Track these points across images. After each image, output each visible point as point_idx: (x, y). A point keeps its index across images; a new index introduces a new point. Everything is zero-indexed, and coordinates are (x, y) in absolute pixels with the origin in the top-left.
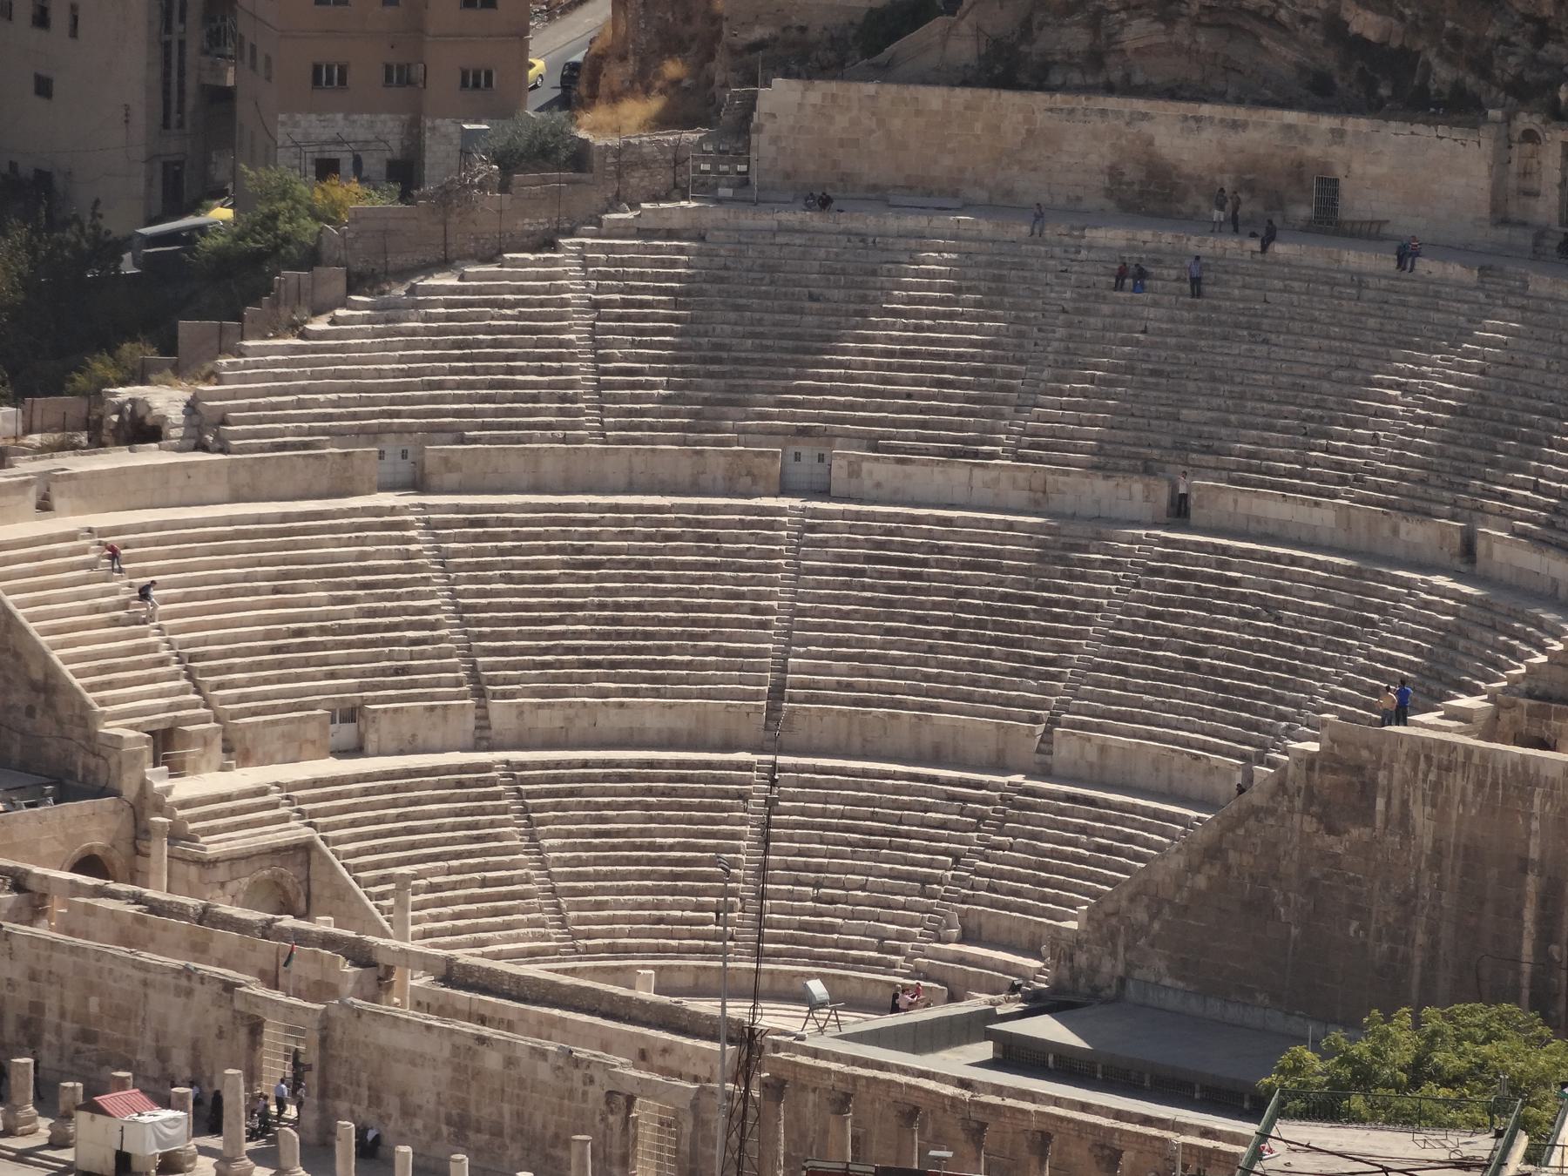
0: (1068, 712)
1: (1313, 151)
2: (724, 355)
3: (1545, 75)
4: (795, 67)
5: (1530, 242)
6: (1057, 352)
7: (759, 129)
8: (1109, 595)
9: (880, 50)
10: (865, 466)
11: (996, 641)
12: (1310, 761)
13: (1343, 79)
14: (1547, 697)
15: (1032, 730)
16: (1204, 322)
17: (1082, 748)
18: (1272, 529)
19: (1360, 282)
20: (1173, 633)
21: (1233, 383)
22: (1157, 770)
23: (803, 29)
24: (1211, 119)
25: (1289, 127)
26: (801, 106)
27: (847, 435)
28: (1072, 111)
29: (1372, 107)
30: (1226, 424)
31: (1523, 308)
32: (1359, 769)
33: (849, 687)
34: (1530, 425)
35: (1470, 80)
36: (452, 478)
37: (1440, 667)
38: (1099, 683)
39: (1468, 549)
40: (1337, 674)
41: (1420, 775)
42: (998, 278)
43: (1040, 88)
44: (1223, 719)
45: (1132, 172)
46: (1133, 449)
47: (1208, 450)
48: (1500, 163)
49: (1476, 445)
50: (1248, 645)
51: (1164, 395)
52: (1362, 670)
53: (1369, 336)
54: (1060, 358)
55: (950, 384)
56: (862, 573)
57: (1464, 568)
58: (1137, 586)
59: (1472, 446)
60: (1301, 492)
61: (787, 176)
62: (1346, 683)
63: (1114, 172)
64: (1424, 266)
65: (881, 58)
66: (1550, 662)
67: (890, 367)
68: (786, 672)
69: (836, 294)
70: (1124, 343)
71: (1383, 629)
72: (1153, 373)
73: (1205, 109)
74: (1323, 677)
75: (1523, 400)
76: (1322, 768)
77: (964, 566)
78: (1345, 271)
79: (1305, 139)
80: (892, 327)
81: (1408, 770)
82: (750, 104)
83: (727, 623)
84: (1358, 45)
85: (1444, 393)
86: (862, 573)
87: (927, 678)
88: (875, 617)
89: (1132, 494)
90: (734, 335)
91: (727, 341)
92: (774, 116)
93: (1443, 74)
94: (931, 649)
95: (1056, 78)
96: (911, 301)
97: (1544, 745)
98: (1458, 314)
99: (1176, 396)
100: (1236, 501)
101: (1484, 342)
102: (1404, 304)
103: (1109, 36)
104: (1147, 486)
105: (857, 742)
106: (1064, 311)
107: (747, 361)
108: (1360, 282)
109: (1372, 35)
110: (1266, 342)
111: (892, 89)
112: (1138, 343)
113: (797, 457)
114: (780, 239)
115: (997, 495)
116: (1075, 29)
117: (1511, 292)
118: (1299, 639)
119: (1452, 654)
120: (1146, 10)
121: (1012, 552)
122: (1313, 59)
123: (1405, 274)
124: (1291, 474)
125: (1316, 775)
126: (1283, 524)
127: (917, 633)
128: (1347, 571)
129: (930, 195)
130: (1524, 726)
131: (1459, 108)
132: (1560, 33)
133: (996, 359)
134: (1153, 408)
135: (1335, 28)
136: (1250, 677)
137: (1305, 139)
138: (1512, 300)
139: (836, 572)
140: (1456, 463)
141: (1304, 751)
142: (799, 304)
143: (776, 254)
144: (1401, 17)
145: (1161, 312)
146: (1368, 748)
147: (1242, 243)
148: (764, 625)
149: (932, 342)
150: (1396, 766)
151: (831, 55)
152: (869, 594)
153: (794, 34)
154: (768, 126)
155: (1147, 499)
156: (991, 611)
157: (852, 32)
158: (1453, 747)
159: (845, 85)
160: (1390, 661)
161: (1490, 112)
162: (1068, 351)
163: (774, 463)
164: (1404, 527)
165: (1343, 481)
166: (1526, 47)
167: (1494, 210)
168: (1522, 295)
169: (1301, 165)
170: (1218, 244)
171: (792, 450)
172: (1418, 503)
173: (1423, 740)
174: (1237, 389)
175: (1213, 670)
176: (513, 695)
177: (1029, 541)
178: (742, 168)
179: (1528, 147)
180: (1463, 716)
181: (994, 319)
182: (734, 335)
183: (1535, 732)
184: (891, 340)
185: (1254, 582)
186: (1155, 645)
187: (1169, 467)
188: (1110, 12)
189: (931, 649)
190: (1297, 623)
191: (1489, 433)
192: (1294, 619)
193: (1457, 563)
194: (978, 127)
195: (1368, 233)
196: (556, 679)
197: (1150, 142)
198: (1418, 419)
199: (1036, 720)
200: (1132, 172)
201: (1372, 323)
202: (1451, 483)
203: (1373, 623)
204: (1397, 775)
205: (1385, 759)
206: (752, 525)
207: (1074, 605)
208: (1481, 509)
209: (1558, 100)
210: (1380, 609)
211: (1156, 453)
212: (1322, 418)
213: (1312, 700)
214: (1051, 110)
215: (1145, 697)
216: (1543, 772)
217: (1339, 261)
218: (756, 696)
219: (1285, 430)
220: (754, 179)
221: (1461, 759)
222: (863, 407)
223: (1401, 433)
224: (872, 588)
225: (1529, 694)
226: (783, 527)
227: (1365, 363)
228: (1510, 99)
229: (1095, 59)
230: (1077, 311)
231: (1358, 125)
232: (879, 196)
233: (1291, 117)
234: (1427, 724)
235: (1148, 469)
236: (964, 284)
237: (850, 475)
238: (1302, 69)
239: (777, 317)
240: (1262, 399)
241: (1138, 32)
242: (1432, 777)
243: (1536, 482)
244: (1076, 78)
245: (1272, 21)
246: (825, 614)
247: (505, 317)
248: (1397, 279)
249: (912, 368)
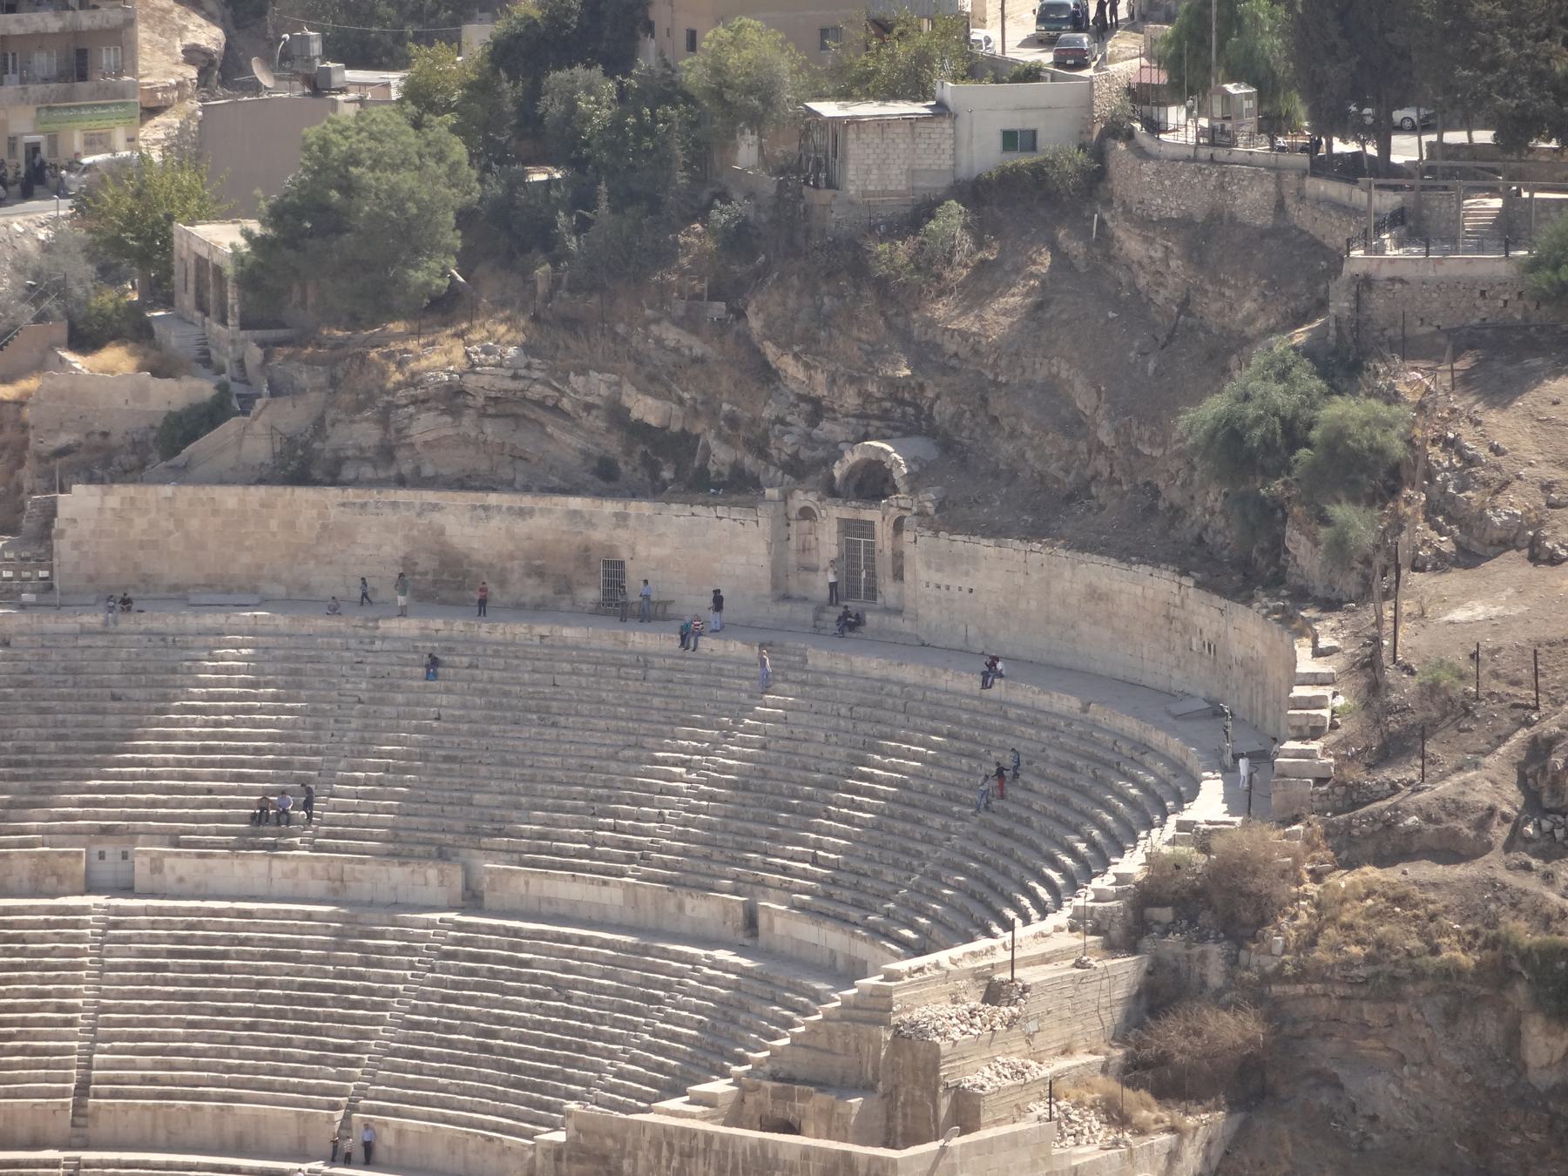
0: (366, 1098)
1: (599, 535)
2: (27, 757)
3: (820, 453)
4: (98, 472)
5: (810, 617)
6: (353, 743)
7: (61, 533)
8: (404, 980)
9: (177, 452)
10: (168, 862)
11: (296, 1030)
12: (557, 1152)
13: (626, 463)
14: (791, 1079)
15: (330, 1117)
16: (495, 707)
18: (563, 909)
19: (646, 662)
20: (468, 1017)
21: (524, 766)
22: (453, 1153)
23: (105, 435)
24: (499, 508)
25: (574, 514)
26: (101, 510)
27: (150, 832)
28: (364, 505)
29: (655, 490)
30: (518, 807)
31: (803, 683)
32: (604, 1158)
33: (154, 1081)
34: (809, 798)
35: (749, 461)
37: (721, 1042)
38: (396, 1068)
39: (751, 922)
40: (624, 1052)
41: (664, 1162)
42: (295, 672)
43: (333, 484)
44: (516, 1100)
45: (425, 563)
46: (428, 835)
47: (500, 833)
48: (779, 541)
49: (757, 819)
50: (539, 1025)
51: (456, 780)
52: (648, 1047)
53: (655, 716)
54: (355, 748)
55: (250, 778)
56: (165, 968)
57: (747, 942)
58: (432, 970)
59: (754, 820)
60: (590, 872)
61: (90, 579)
62: (631, 1061)
63: (408, 563)
64: (708, 644)
65: (178, 460)
66: (792, 1044)
67: (190, 763)
68: (90, 1067)
69: (138, 693)
70: (418, 730)
71: (669, 1005)
72: (447, 759)
73: (493, 499)
74: (611, 1055)
75: (803, 774)
76: (569, 1159)
77: (265, 957)
78: (630, 652)
79: (590, 524)
80: (193, 723)
81: (651, 1157)
82: (51, 511)
83: (34, 1022)
84: (640, 430)
85: (726, 769)
86: (165, 968)
87: (229, 1069)
88: (179, 1010)
89: (429, 878)
90: (38, 738)
91: (28, 743)
92: (74, 521)
93: (722, 456)
94: (233, 1040)
95: (348, 473)
96: (211, 697)
97: (790, 1128)
98: (740, 690)
99: (468, 781)
100: (527, 883)
101: (764, 718)
102: (687, 682)
103: (399, 431)
104: (441, 871)
105: (161, 1135)
106: (360, 701)
107: (51, 764)
108: (646, 662)
109: (653, 420)
110: (554, 725)
111: (189, 490)
112: (431, 731)
113: (102, 856)
114: (81, 642)
115: (296, 885)
116: (365, 425)
117: (790, 668)
118: (587, 1018)
119: (733, 1028)
120: (432, 404)
121: (311, 941)
122: (598, 445)
123: (689, 653)
124: (580, 854)
125: (564, 1166)
126: (574, 904)
127: (219, 1026)
128: (632, 949)
129: (229, 592)
130: (769, 1107)
131: (738, 487)
132: (834, 411)
133: (293, 752)
134: (446, 794)
135: (617, 415)
136: (541, 1058)
137: (590, 524)
138: (791, 675)
139: (140, 967)
140: (738, 838)
141: (551, 1142)
142: (102, 704)
143: (79, 657)
144: (681, 401)
145: (453, 699)
146: (612, 1136)
147: (531, 628)
148: (70, 1023)
149: (231, 737)
150: (640, 1154)
151: (133, 459)
152: (171, 989)
153: (97, 439)
154: (70, 531)
155: (441, 884)
156: (290, 1000)
157: (153, 435)
158: (693, 1134)
159: (142, 488)
160: (675, 1037)
161: (768, 491)
162: (363, 741)
163: (79, 862)
164: (689, 903)
165: (630, 860)
166: (800, 425)
167: (775, 587)
168: (803, 670)
170: (508, 630)
171: (96, 849)
172: (701, 879)
173: (665, 1128)
174: (527, 771)
175: (506, 1051)
177: (326, 931)
178: (43, 574)
179: (806, 523)
180: (708, 1101)
181: (291, 711)
182: (38, 738)
183: (779, 1114)
184: (192, 736)
185: (545, 962)
186: (450, 1029)
187: (464, 852)
188: (398, 407)
189: (233, 1040)
190: (586, 1002)
191: (763, 807)
192: (582, 997)
193: (741, 938)
194: (274, 524)
195: (650, 612)
197: (442, 533)
198: (701, 796)
199: (335, 1107)
200: (425, 563)
201: (657, 702)
202: (733, 858)
203: (659, 1000)
204: (642, 1163)
205: (629, 1147)
206: (57, 925)
207: (370, 992)
208: (761, 883)
209: (832, 477)
210: (666, 986)
211: (449, 838)
212: (609, 797)
213: (600, 1078)
214: (344, 505)
215: (441, 1080)
216: (781, 1156)
217: (625, 643)
218: (63, 1093)
219: (575, 810)
220: (56, 583)
221: (701, 1145)
222: (165, 804)
223: (685, 810)
224: (175, 982)
225: (774, 1077)
226: (86, 925)
227: (650, 742)
228: (787, 477)
229: (387, 453)
230: (372, 701)
231: (642, 508)
232: (180, 595)
233: (575, 503)
234: (673, 1113)
235: (442, 854)
236: (262, 679)
237: (153, 871)
238: (586, 455)
239: (81, 718)
240: (552, 781)
242: (675, 1164)
243: (815, 856)
244: (368, 472)
245: (556, 409)
246: (129, 1009)
248: (681, 658)
249: (212, 764)
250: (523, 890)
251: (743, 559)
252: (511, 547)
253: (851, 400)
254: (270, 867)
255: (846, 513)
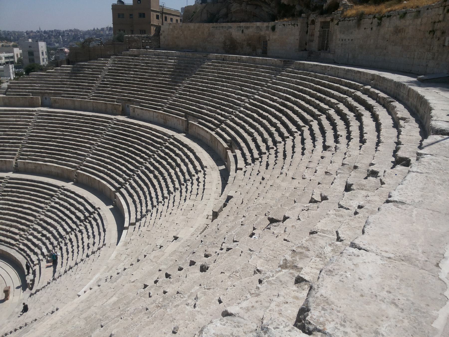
1: (262, 33)
7: (161, 35)
10: (136, 109)
25: (258, 27)
28: (217, 27)
36: (57, 105)
45: (228, 43)
63: (225, 43)
79: (261, 30)
171: (127, 105)
176: (25, 159)
196: (38, 156)
229: (226, 15)
233: (258, 24)
241: (235, 7)
247: (89, 71)
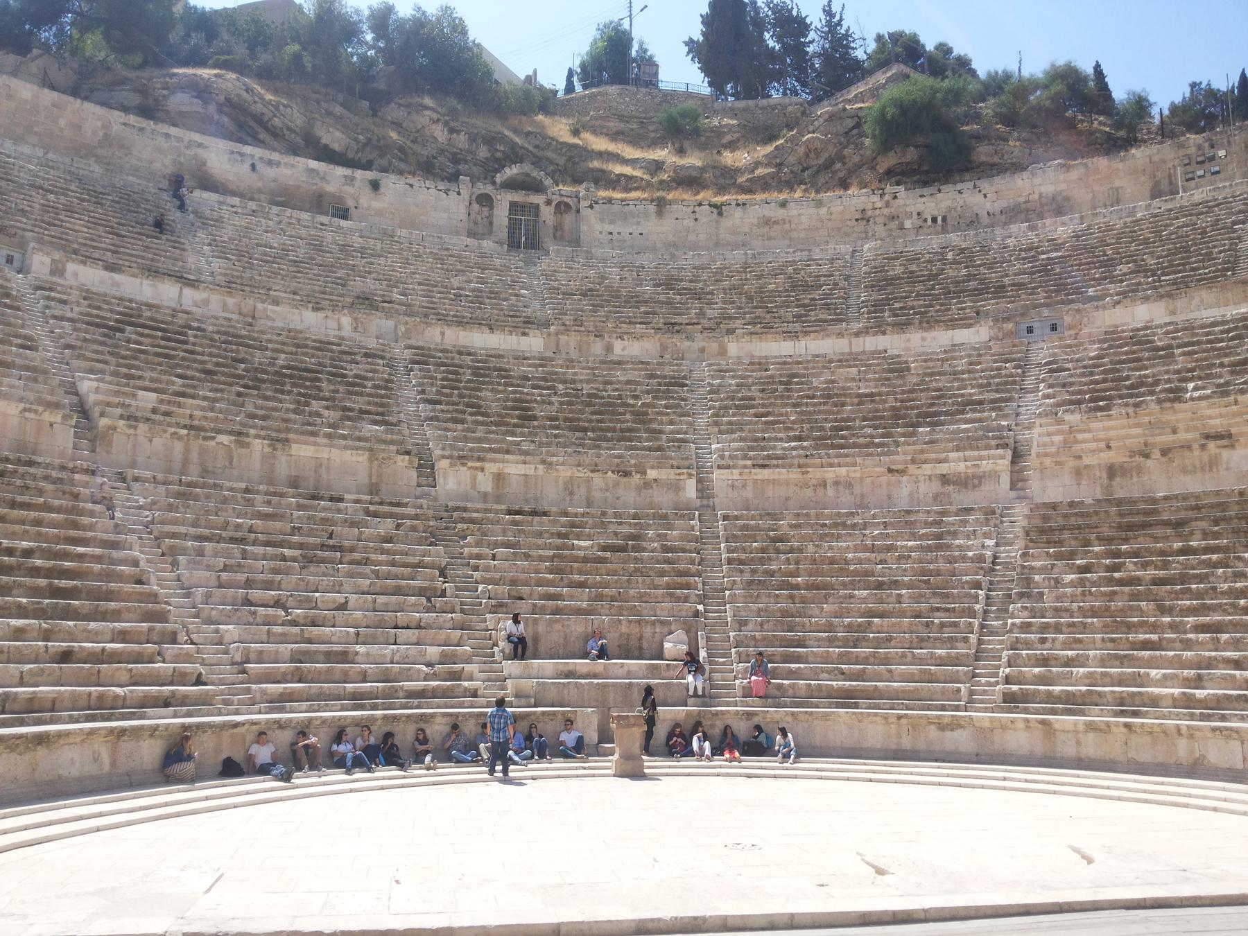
1: (330, 188)
17: (474, 479)
22: (571, 493)
25: (313, 170)
28: (142, 130)
73: (247, 149)
79: (323, 179)
100: (443, 334)
109: (336, 147)
137: (323, 179)
144: (356, 140)
169: (320, 196)
194: (62, 122)
197: (204, 164)
214: (125, 124)
233: (314, 164)
250: (438, 339)
251: (446, 215)
252: (260, 184)
253: (483, 153)
254: (181, 295)
255: (518, 197)
